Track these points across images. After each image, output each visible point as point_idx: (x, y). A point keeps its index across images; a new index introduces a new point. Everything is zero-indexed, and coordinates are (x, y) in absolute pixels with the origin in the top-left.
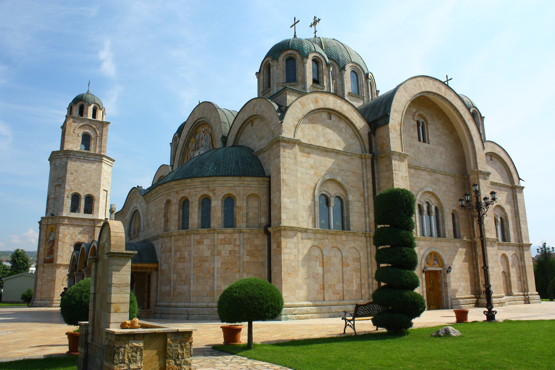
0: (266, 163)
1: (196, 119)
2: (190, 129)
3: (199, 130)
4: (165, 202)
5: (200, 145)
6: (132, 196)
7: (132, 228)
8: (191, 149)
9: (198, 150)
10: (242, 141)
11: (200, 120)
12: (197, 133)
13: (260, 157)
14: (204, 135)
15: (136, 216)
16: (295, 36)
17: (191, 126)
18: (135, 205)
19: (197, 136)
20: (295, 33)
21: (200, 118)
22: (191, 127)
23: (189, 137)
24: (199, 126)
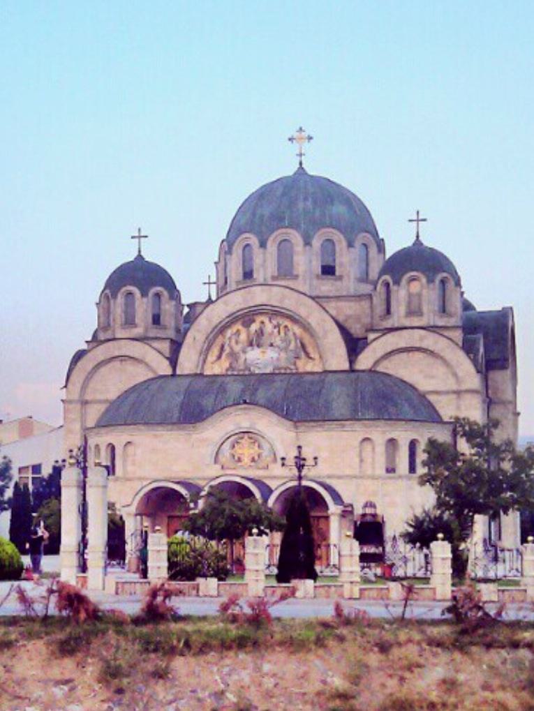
0: (443, 407)
2: (238, 311)
3: (259, 319)
4: (360, 439)
5: (266, 340)
8: (233, 341)
9: (259, 346)
10: (387, 368)
12: (254, 321)
13: (432, 398)
14: (276, 331)
15: (242, 438)
17: (238, 307)
18: (245, 424)
19: (254, 327)
24: (261, 313)
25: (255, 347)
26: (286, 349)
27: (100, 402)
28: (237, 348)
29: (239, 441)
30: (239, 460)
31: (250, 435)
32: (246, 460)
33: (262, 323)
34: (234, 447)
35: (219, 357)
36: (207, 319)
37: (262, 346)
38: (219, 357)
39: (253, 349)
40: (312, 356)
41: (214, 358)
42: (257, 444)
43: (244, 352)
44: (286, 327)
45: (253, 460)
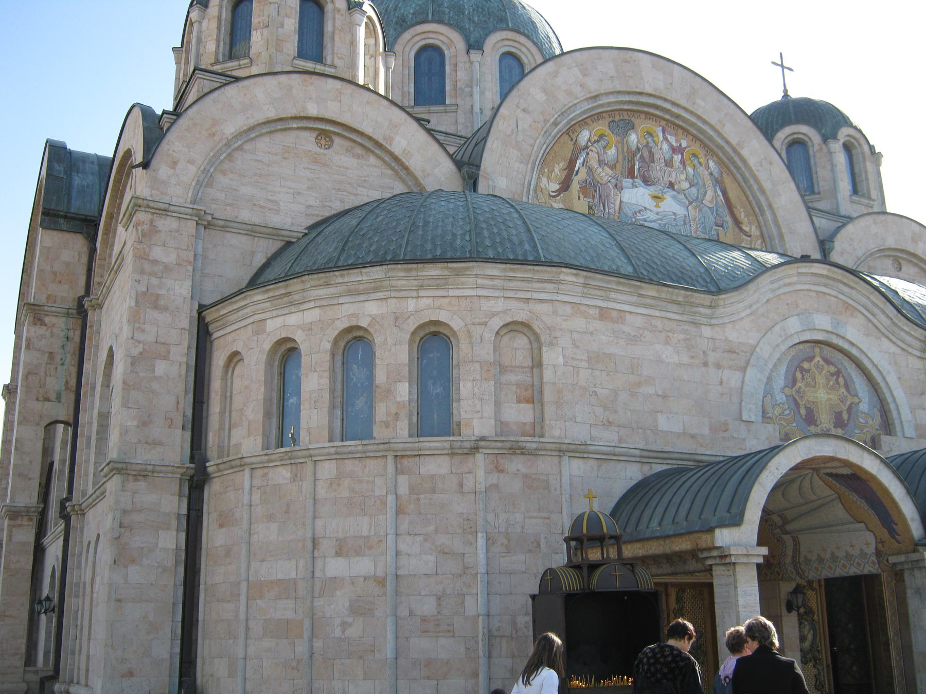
1: (648, 90)
2: (608, 94)
3: (643, 125)
6: (795, 279)
7: (780, 398)
8: (593, 155)
9: (647, 181)
11: (659, 103)
14: (677, 158)
15: (810, 359)
16: (785, 91)
17: (608, 86)
18: (823, 321)
19: (633, 138)
20: (785, 85)
21: (674, 104)
22: (612, 93)
23: (584, 112)
25: (638, 181)
26: (697, 202)
27: (253, 231)
28: (604, 174)
29: (806, 365)
30: (810, 419)
31: (828, 351)
32: (825, 420)
33: (650, 134)
34: (794, 381)
35: (565, 186)
36: (545, 91)
37: (653, 184)
38: (565, 186)
39: (634, 186)
40: (746, 228)
41: (557, 187)
42: (841, 380)
43: (619, 187)
44: (694, 155)
45: (839, 422)
